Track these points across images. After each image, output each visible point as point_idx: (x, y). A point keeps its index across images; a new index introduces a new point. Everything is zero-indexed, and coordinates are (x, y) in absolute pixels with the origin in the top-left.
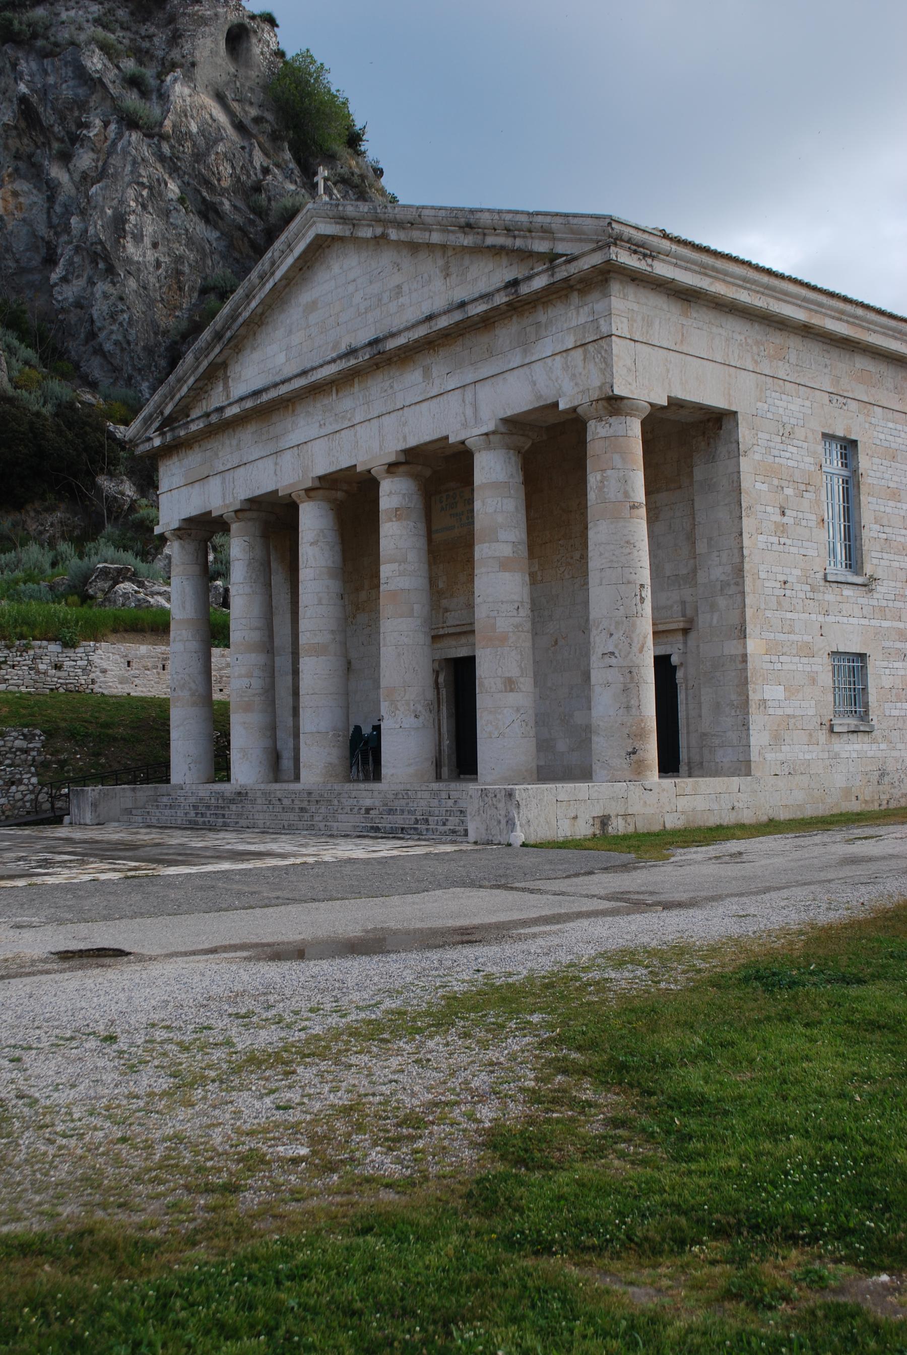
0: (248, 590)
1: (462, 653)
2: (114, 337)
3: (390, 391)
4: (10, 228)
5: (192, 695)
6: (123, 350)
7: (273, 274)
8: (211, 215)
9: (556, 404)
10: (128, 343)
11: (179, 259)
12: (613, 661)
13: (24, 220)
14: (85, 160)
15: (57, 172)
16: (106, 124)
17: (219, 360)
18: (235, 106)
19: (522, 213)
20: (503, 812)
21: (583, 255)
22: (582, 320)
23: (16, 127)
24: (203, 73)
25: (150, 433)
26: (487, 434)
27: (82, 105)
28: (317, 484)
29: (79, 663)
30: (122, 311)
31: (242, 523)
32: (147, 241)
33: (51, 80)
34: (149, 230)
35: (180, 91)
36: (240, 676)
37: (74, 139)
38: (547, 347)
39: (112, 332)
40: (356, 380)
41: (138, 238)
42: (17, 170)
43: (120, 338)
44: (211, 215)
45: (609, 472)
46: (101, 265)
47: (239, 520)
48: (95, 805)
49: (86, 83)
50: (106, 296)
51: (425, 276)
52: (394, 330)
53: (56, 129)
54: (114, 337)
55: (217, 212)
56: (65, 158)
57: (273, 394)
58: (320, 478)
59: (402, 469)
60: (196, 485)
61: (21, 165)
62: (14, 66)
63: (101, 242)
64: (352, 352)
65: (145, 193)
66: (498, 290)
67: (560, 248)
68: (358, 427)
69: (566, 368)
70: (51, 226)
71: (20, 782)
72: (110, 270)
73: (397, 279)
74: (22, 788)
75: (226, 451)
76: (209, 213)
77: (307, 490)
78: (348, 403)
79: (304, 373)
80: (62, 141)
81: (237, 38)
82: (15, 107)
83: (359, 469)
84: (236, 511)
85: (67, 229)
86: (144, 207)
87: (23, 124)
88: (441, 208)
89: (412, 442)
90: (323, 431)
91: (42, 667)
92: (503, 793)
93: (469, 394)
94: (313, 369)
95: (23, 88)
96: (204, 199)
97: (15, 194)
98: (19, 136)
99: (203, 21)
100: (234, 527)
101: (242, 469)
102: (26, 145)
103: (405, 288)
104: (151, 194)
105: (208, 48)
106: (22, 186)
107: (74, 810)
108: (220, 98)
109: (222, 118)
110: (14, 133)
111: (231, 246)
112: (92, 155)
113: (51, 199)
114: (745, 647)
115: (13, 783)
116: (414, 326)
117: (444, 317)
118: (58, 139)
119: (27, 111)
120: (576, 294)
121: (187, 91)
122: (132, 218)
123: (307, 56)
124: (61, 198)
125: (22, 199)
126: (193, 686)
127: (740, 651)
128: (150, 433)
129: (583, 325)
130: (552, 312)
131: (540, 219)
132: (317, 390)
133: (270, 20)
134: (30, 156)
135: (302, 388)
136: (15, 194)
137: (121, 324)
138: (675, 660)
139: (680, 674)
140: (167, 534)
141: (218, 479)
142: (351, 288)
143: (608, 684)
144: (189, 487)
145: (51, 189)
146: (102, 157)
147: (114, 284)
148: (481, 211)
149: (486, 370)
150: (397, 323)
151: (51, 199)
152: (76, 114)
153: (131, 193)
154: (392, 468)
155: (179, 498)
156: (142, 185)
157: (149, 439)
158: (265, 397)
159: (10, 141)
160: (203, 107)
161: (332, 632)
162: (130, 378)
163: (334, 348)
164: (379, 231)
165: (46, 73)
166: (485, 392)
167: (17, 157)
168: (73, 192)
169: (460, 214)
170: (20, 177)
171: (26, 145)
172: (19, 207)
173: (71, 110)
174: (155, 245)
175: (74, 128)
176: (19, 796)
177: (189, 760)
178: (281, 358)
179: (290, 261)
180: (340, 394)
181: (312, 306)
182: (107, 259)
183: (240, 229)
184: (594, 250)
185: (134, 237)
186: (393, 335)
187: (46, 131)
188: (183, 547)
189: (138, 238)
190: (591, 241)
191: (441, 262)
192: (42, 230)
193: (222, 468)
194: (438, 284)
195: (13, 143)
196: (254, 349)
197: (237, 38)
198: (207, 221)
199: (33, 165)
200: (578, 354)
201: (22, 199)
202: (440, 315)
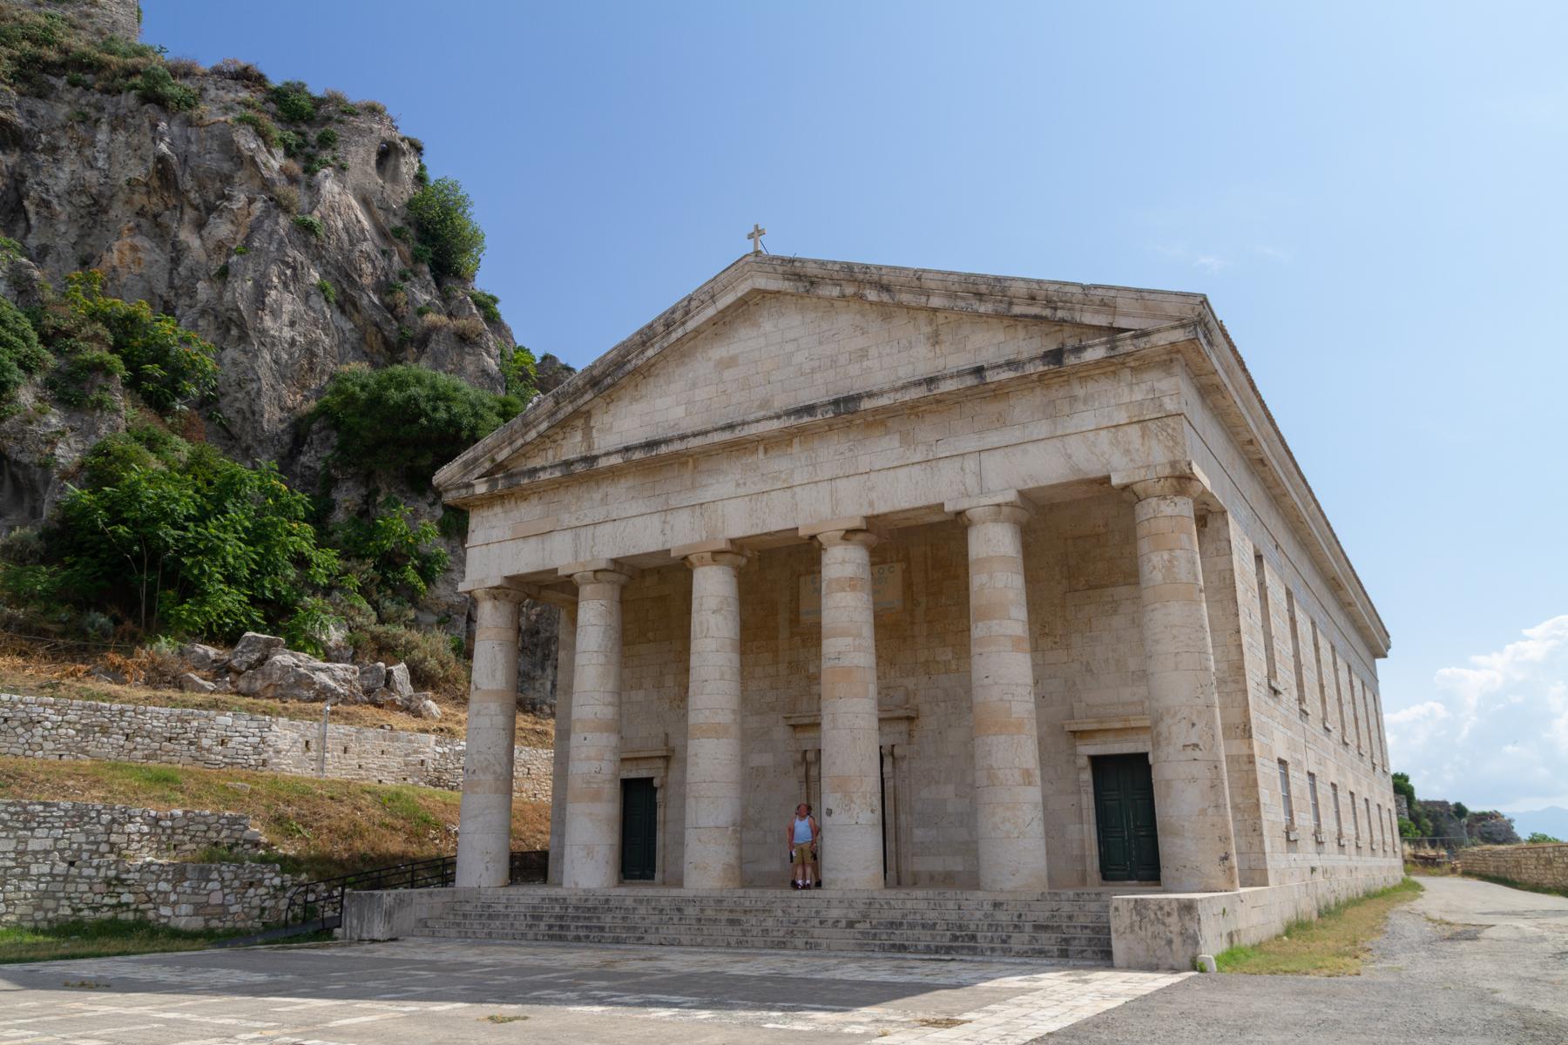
0: (602, 659)
2: (237, 405)
3: (848, 454)
4: (123, 280)
5: (497, 779)
6: (245, 419)
7: (683, 324)
8: (348, 307)
9: (1108, 478)
10: (253, 413)
11: (315, 342)
12: (1197, 754)
13: (141, 275)
14: (222, 229)
15: (187, 236)
16: (251, 201)
17: (584, 409)
18: (381, 215)
19: (1073, 284)
20: (1176, 928)
21: (1159, 331)
22: (1138, 395)
23: (146, 185)
24: (353, 176)
25: (471, 478)
26: (999, 505)
27: (227, 179)
28: (729, 547)
29: (251, 740)
30: (252, 380)
31: (600, 586)
32: (286, 318)
33: (194, 148)
34: (288, 307)
35: (330, 186)
36: (588, 758)
37: (211, 209)
38: (1087, 419)
39: (236, 399)
40: (796, 440)
41: (275, 314)
42: (138, 226)
43: (244, 407)
44: (348, 307)
45: (1178, 552)
46: (234, 332)
47: (597, 581)
48: (389, 915)
49: (232, 159)
50: (235, 363)
51: (904, 342)
52: (875, 389)
53: (192, 195)
54: (237, 405)
55: (355, 305)
56: (200, 225)
57: (677, 446)
58: (732, 541)
59: (860, 536)
60: (533, 541)
61: (143, 221)
62: (154, 127)
63: (238, 310)
64: (810, 410)
65: (289, 272)
66: (1031, 360)
67: (1121, 322)
68: (797, 489)
70: (171, 286)
71: (261, 882)
72: (243, 338)
73: (860, 342)
74: (262, 891)
75: (587, 505)
76: (346, 305)
77: (715, 553)
78: (791, 464)
79: (731, 427)
80: (196, 208)
81: (387, 154)
82: (151, 165)
83: (801, 533)
84: (596, 572)
85: (192, 294)
86: (286, 286)
87: (155, 183)
88: (951, 273)
89: (881, 508)
90: (742, 491)
91: (206, 742)
92: (1175, 905)
93: (970, 464)
94: (744, 423)
95: (163, 147)
96: (344, 291)
97: (134, 248)
98: (148, 193)
99: (360, 132)
100: (586, 591)
101: (608, 527)
102: (154, 204)
103: (873, 352)
104: (295, 275)
105: (360, 157)
106: (142, 241)
107: (351, 920)
108: (365, 202)
109: (366, 224)
110: (144, 189)
111: (362, 339)
112: (230, 226)
113: (175, 261)
114: (1250, 747)
115: (251, 884)
116: (904, 387)
117: (949, 382)
118: (192, 206)
119: (164, 172)
120: (1128, 371)
121: (336, 189)
122: (273, 293)
123: (455, 187)
124: (187, 262)
125: (140, 255)
126: (498, 769)
127: (1245, 751)
128: (471, 478)
129: (1141, 404)
130: (1091, 387)
131: (1100, 292)
133: (418, 149)
134: (156, 216)
135: (719, 444)
136: (134, 248)
137: (248, 393)
138: (656, 783)
139: (659, 795)
140: (479, 593)
141: (568, 536)
142: (790, 347)
143: (1194, 780)
144: (520, 542)
145: (177, 253)
146: (243, 231)
147: (245, 352)
148: (1013, 279)
149: (993, 439)
150: (878, 380)
151: (175, 261)
152: (218, 185)
153: (274, 269)
154: (849, 534)
155: (496, 551)
156: (287, 264)
157: (469, 486)
158: (664, 449)
159: (136, 197)
160: (350, 207)
161: (734, 711)
162: (248, 448)
163: (761, 407)
165: (189, 141)
166: (993, 463)
167: (141, 213)
168: (203, 258)
169: (979, 281)
170: (141, 233)
171: (154, 204)
172: (138, 262)
173: (213, 180)
174: (292, 324)
175: (212, 198)
176: (256, 902)
177: (487, 858)
178: (680, 412)
179: (710, 312)
180: (771, 453)
181: (731, 362)
182: (242, 326)
183: (376, 325)
184: (1173, 328)
185: (272, 312)
186: (870, 395)
187: (180, 194)
188: (495, 607)
189: (275, 314)
190: (1171, 317)
191: (927, 330)
192: (162, 288)
194: (922, 351)
195: (139, 199)
196: (634, 400)
197: (387, 154)
198: (343, 312)
199: (158, 225)
200: (1135, 431)
201: (140, 255)
202: (944, 378)
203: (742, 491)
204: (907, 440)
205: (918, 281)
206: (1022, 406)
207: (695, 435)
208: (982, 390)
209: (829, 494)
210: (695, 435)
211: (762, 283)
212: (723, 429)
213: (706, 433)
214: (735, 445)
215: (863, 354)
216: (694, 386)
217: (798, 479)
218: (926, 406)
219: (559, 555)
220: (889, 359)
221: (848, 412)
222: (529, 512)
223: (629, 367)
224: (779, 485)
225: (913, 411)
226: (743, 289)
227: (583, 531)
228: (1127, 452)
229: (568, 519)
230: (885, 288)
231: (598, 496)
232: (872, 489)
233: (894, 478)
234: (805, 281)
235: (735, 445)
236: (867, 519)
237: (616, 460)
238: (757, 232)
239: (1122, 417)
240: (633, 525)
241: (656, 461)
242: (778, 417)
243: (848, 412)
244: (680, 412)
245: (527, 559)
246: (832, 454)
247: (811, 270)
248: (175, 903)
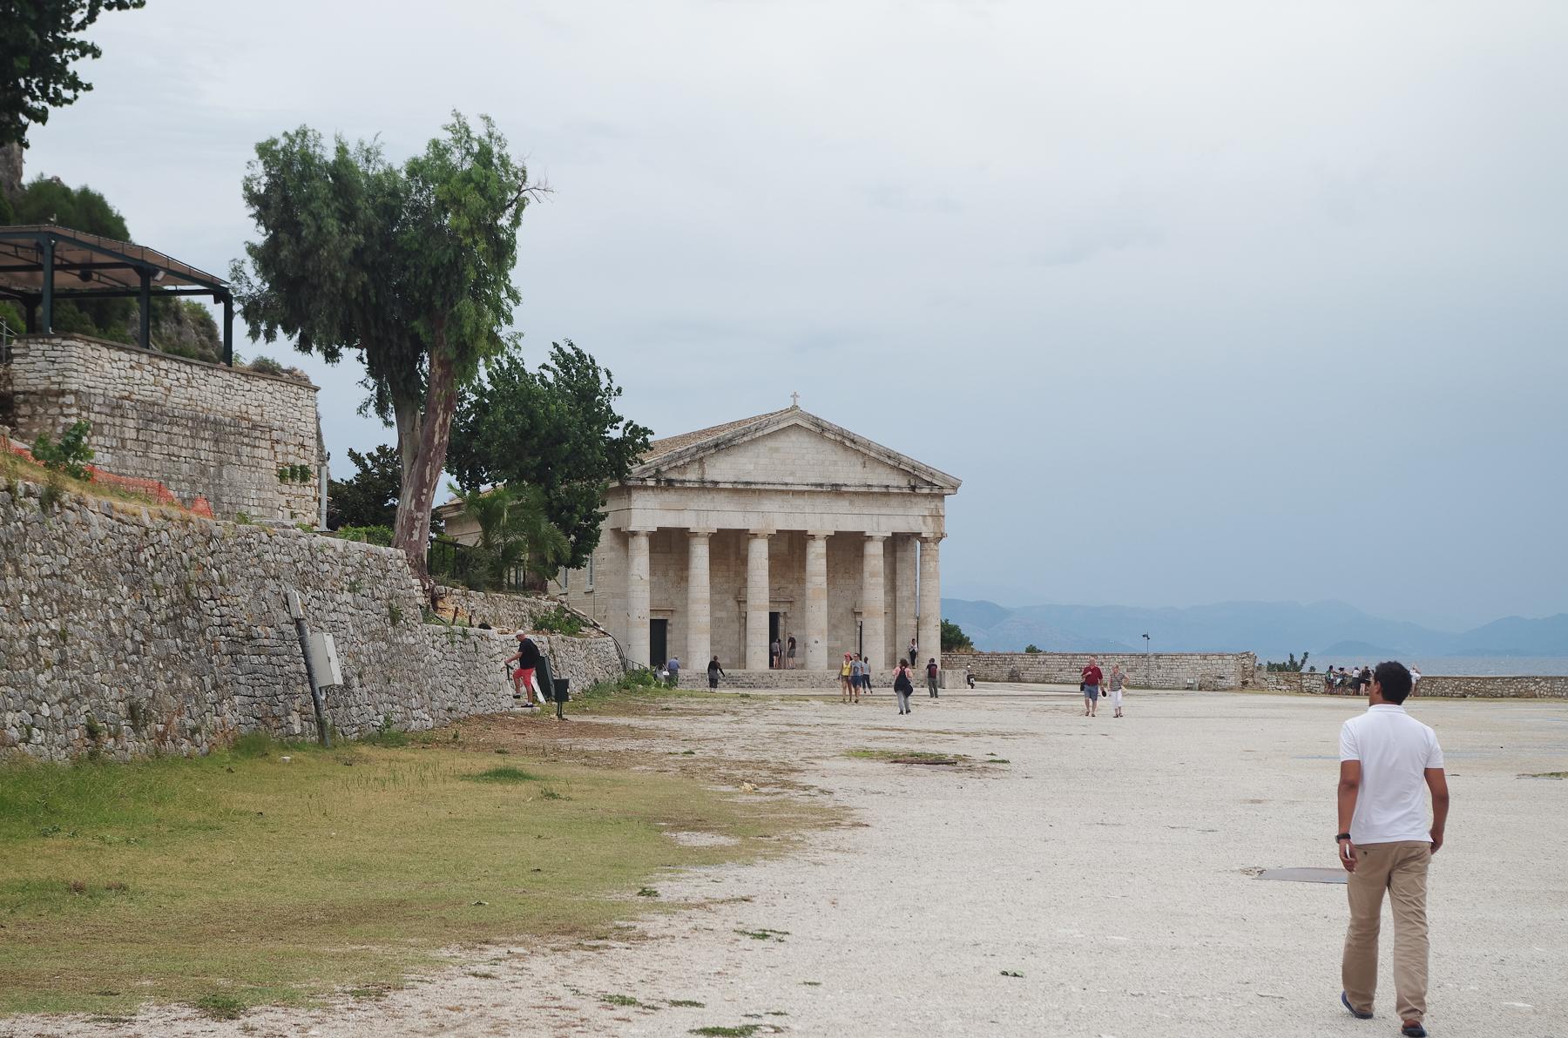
64: (821, 485)
73: (834, 458)
75: (704, 501)
166: (883, 519)
179: (776, 428)
181: (777, 450)
204: (851, 503)
205: (868, 445)
206: (894, 502)
208: (886, 493)
209: (822, 520)
214: (785, 492)
215: (835, 463)
218: (867, 494)
220: (850, 472)
221: (836, 491)
222: (670, 497)
226: (792, 422)
229: (692, 505)
230: (853, 441)
233: (846, 518)
234: (819, 430)
235: (785, 492)
238: (795, 396)
240: (730, 516)
241: (744, 490)
243: (836, 491)
245: (671, 521)
246: (821, 504)
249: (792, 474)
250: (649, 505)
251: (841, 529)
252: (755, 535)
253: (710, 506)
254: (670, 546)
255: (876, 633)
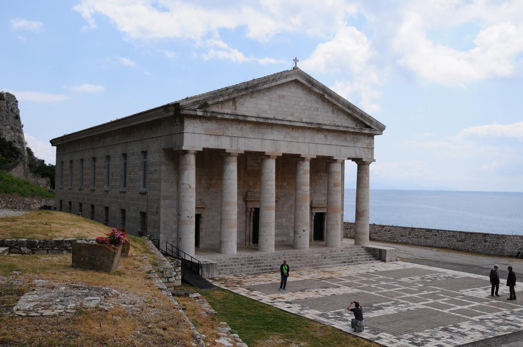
1: (257, 206)
22: (368, 142)
38: (359, 144)
64: (311, 123)
67: (372, 126)
69: (364, 151)
73: (316, 106)
90: (285, 139)
101: (243, 139)
103: (319, 110)
132: (294, 128)
141: (228, 139)
142: (299, 100)
144: (208, 136)
164: (321, 93)
166: (343, 149)
186: (325, 125)
191: (331, 109)
193: (230, 135)
203: (285, 139)
204: (326, 137)
207: (280, 120)
210: (280, 120)
211: (299, 79)
212: (288, 121)
213: (283, 120)
216: (271, 100)
217: (301, 140)
219: (224, 144)
222: (212, 126)
223: (258, 88)
224: (295, 141)
225: (329, 131)
226: (294, 78)
227: (234, 139)
228: (365, 154)
231: (239, 127)
232: (318, 148)
236: (317, 156)
237: (254, 120)
239: (365, 146)
242: (303, 123)
244: (266, 107)
245: (212, 143)
246: (308, 136)
247: (315, 82)
248: (175, 276)
249: (292, 115)
250: (198, 130)
251: (320, 154)
252: (269, 157)
253: (240, 134)
254: (211, 162)
255: (337, 223)
